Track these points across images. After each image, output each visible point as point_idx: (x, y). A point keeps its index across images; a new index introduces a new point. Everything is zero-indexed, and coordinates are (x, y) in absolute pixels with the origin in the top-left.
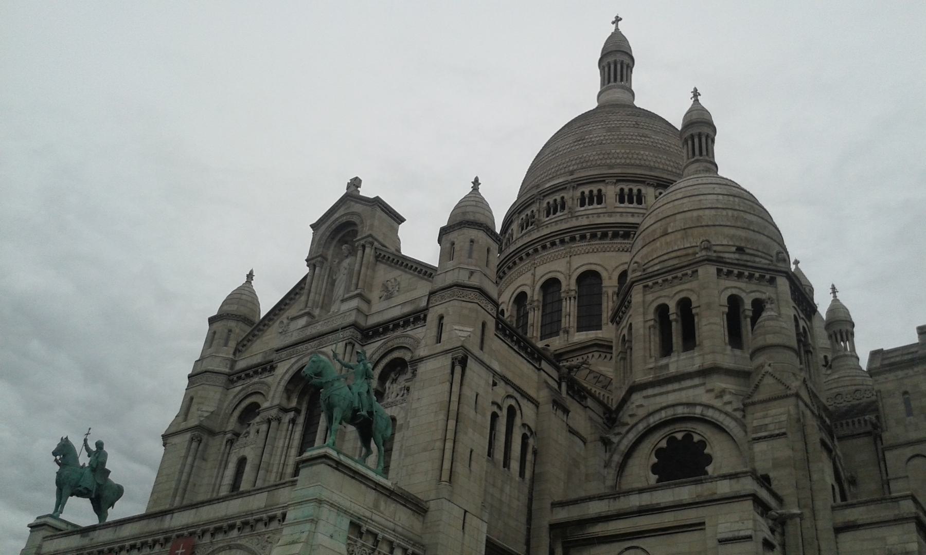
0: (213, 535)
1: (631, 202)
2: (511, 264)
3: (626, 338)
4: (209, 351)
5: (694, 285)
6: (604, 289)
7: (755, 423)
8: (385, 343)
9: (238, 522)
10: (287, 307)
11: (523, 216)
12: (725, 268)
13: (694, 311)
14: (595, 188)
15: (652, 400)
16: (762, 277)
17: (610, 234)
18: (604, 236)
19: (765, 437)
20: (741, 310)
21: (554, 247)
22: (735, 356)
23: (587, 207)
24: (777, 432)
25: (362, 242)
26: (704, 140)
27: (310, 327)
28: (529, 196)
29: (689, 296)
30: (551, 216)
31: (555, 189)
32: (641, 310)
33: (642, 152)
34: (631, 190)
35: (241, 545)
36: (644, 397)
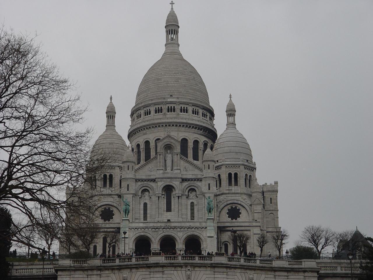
2: (154, 127)
5: (239, 170)
6: (189, 146)
7: (255, 209)
8: (189, 184)
9: (195, 228)
10: (150, 163)
12: (246, 167)
13: (238, 177)
17: (192, 127)
18: (190, 127)
23: (182, 113)
27: (166, 174)
28: (160, 101)
30: (170, 113)
31: (171, 103)
32: (225, 173)
34: (196, 109)
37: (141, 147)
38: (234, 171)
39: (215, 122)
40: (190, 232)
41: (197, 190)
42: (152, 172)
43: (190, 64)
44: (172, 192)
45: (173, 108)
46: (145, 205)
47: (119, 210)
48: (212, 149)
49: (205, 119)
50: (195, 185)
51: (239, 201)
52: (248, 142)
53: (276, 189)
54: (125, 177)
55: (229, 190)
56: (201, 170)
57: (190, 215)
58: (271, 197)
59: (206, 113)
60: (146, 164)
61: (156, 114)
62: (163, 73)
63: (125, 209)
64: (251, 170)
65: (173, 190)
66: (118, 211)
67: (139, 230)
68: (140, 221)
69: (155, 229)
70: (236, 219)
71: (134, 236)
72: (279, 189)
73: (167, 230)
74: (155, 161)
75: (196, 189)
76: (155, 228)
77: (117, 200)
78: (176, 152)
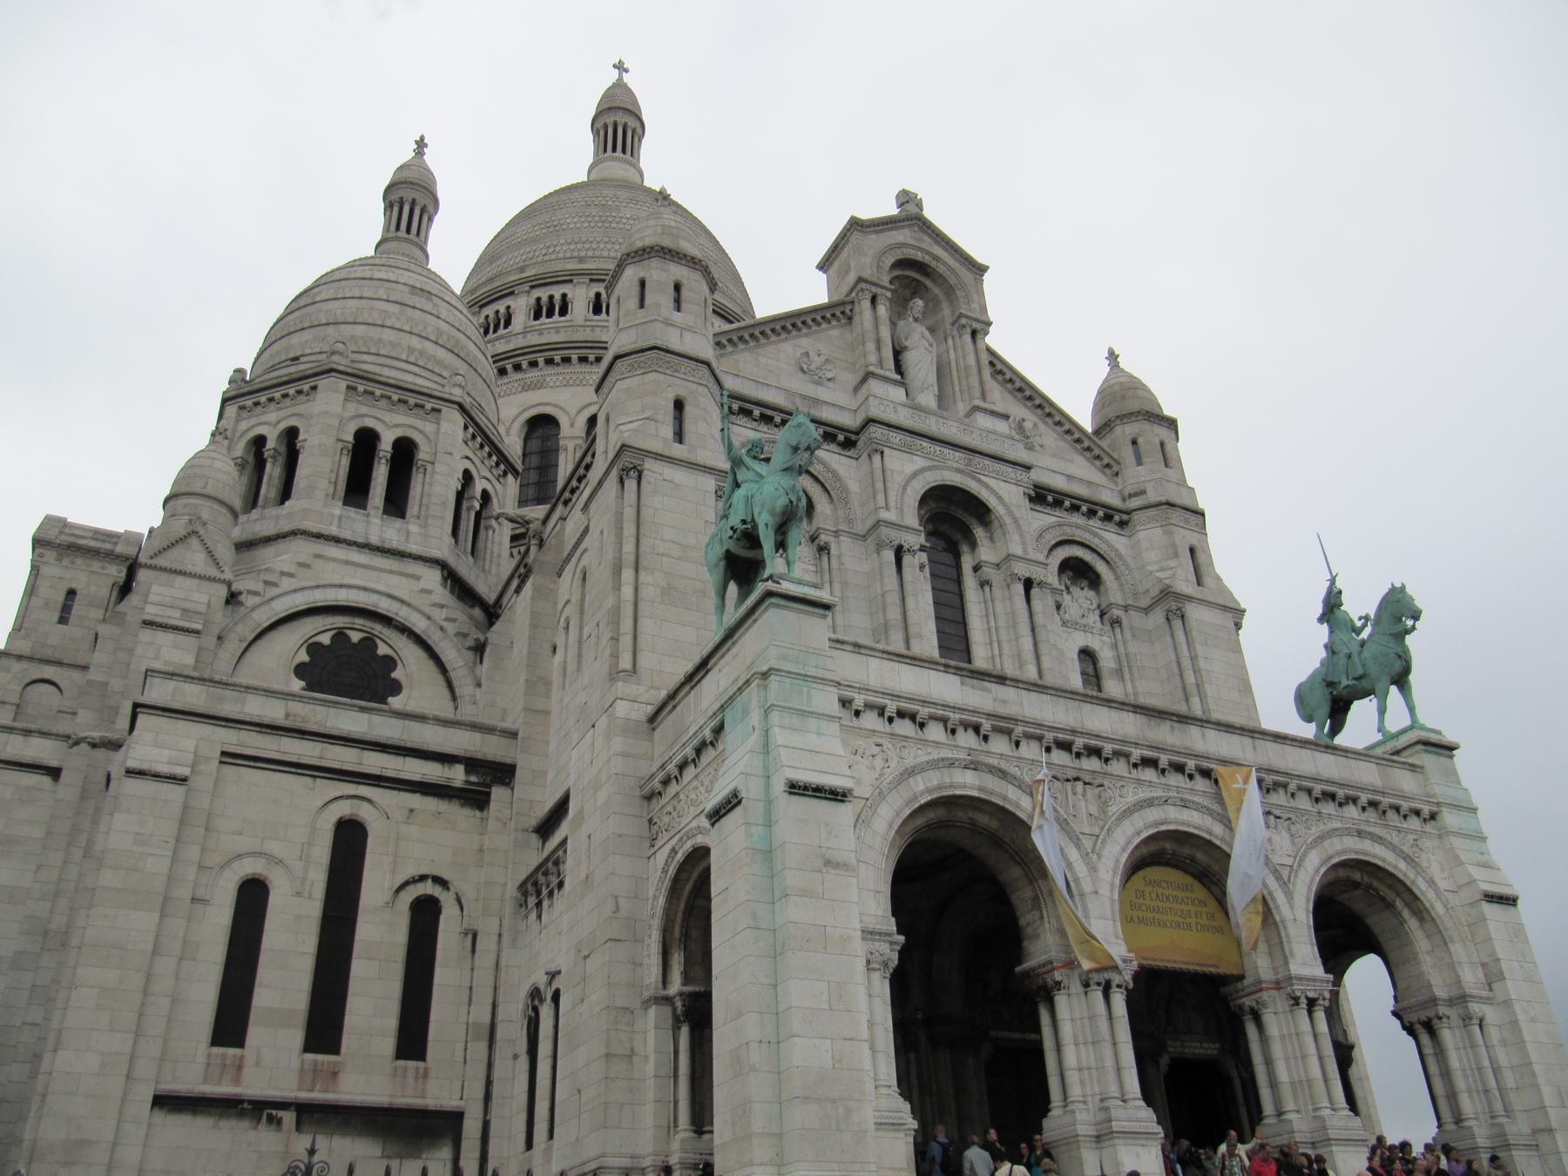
0: (1317, 800)
2: (592, 358)
4: (677, 317)
9: (1364, 798)
10: (805, 330)
27: (933, 419)
35: (1381, 838)
41: (1112, 578)
44: (965, 548)
50: (1095, 542)
54: (659, 343)
56: (1111, 468)
61: (596, 317)
63: (782, 502)
65: (979, 532)
66: (430, 665)
67: (935, 732)
69: (1078, 755)
73: (1175, 779)
74: (835, 333)
75: (1100, 567)
77: (436, 598)
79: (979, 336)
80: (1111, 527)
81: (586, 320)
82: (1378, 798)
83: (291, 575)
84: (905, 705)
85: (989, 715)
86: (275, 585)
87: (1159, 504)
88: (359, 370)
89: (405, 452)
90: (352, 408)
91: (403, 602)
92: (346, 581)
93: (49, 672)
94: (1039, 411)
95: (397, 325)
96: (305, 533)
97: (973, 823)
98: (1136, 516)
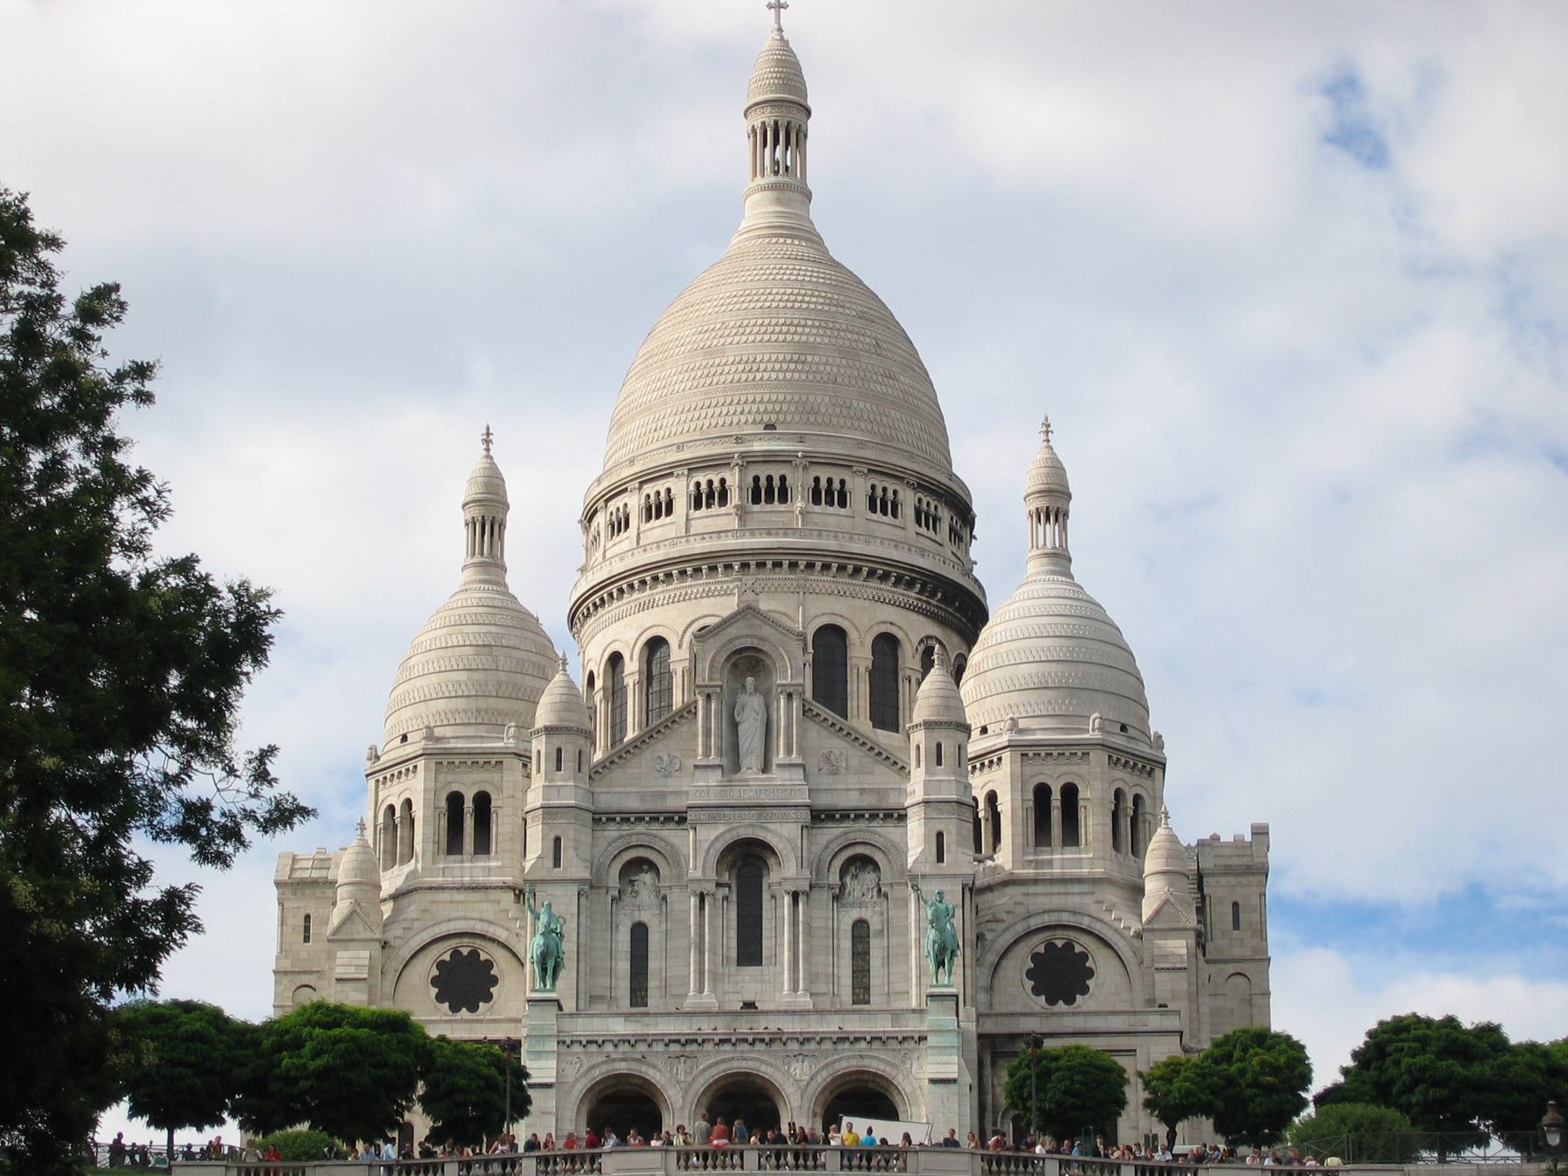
1: (884, 512)
3: (981, 805)
4: (561, 779)
5: (1083, 769)
9: (868, 1038)
10: (660, 736)
11: (702, 478)
12: (1118, 758)
13: (1081, 803)
14: (837, 475)
15: (1032, 900)
16: (1144, 767)
17: (865, 571)
18: (857, 570)
19: (1168, 969)
20: (1122, 806)
21: (777, 570)
22: (1120, 863)
24: (1178, 966)
25: (790, 690)
26: (1061, 518)
29: (1076, 783)
31: (769, 458)
33: (892, 412)
34: (884, 490)
36: (1024, 895)
37: (626, 673)
38: (1064, 774)
39: (975, 551)
40: (847, 1061)
41: (886, 862)
42: (671, 781)
43: (859, 282)
44: (765, 872)
45: (776, 483)
46: (640, 933)
47: (519, 960)
48: (958, 672)
49: (931, 533)
51: (1083, 914)
52: (1130, 638)
53: (1262, 860)
55: (1036, 861)
57: (850, 982)
58: (1235, 898)
59: (936, 508)
60: (644, 741)
61: (698, 513)
62: (732, 324)
64: (1141, 771)
65: (771, 861)
66: (514, 961)
67: (609, 1048)
68: (614, 1010)
69: (683, 1045)
70: (1070, 1001)
71: (581, 1077)
72: (1274, 858)
74: (684, 729)
75: (878, 857)
76: (683, 1039)
78: (784, 682)
79: (794, 697)
80: (890, 823)
81: (687, 520)
82: (879, 1035)
83: (418, 920)
84: (590, 1039)
85: (633, 1035)
86: (410, 929)
87: (918, 804)
88: (440, 749)
89: (483, 801)
90: (442, 777)
91: (490, 922)
92: (454, 915)
93: (306, 979)
94: (848, 739)
95: (466, 693)
96: (421, 888)
97: (631, 1084)
98: (909, 811)
